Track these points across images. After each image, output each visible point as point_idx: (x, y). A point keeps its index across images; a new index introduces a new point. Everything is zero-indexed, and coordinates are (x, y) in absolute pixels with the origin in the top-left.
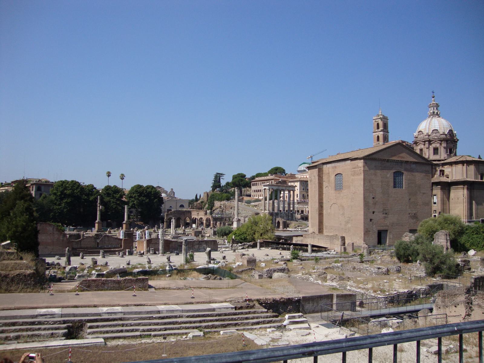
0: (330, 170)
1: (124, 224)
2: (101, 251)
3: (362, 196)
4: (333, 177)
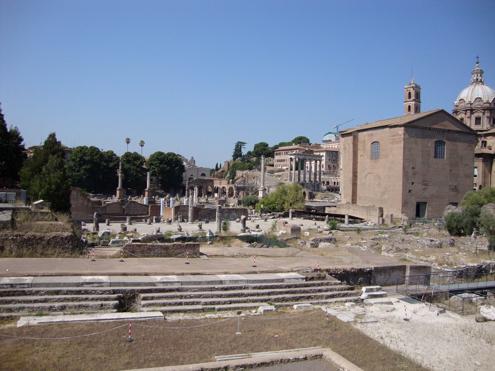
0: (366, 138)
1: (147, 191)
2: (128, 218)
4: (369, 145)
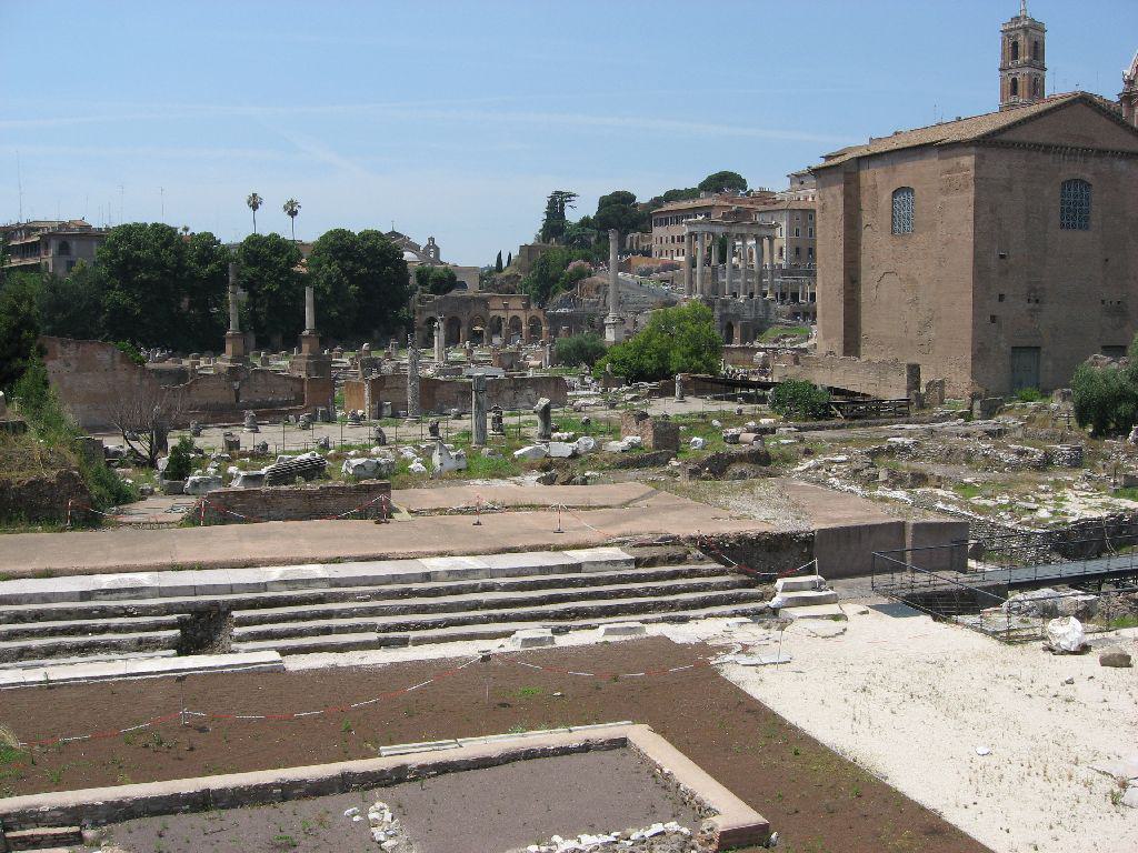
3: (969, 252)
4: (886, 196)
